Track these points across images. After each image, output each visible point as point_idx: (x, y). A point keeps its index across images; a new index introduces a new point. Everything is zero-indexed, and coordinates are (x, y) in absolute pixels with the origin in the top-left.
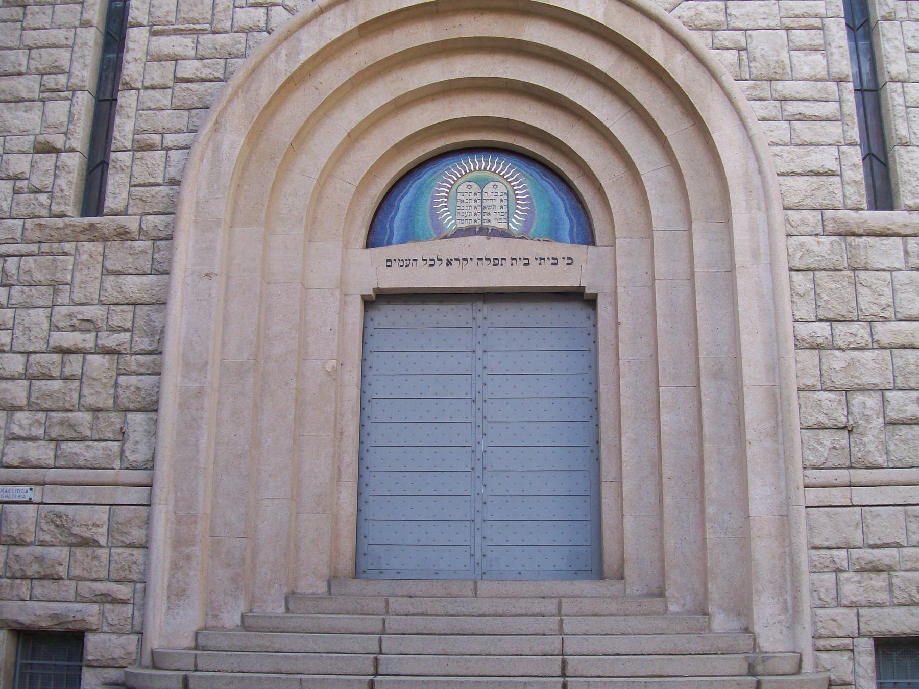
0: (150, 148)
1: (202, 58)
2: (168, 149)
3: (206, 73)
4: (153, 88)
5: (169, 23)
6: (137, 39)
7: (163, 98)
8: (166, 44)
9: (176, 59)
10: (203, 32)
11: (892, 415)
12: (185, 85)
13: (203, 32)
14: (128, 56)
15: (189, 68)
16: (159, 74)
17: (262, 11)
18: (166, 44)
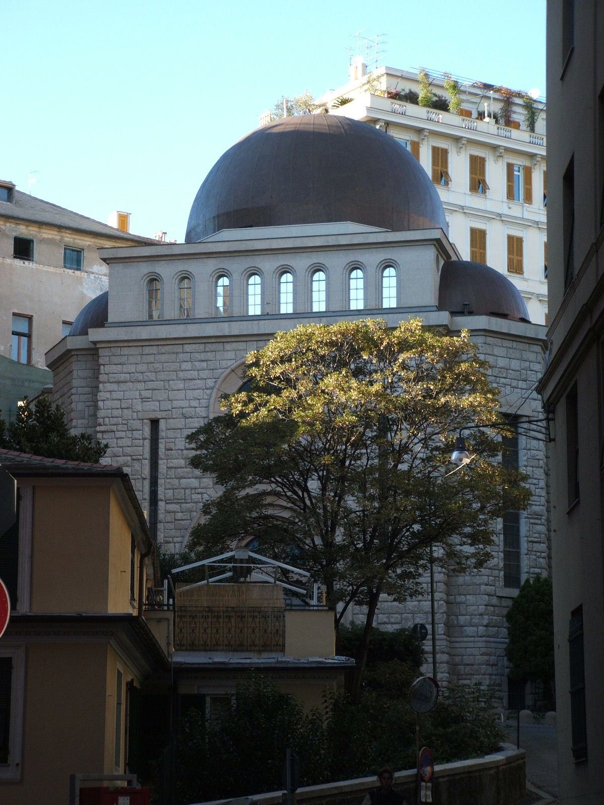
0: (170, 542)
1: (182, 512)
2: (175, 543)
3: (184, 517)
4: (168, 522)
5: (171, 500)
6: (161, 504)
7: (171, 526)
8: (172, 507)
9: (174, 512)
10: (182, 503)
11: (379, 621)
12: (178, 522)
13: (182, 503)
14: (159, 512)
15: (179, 516)
16: (169, 518)
17: (200, 495)
18: (172, 507)
